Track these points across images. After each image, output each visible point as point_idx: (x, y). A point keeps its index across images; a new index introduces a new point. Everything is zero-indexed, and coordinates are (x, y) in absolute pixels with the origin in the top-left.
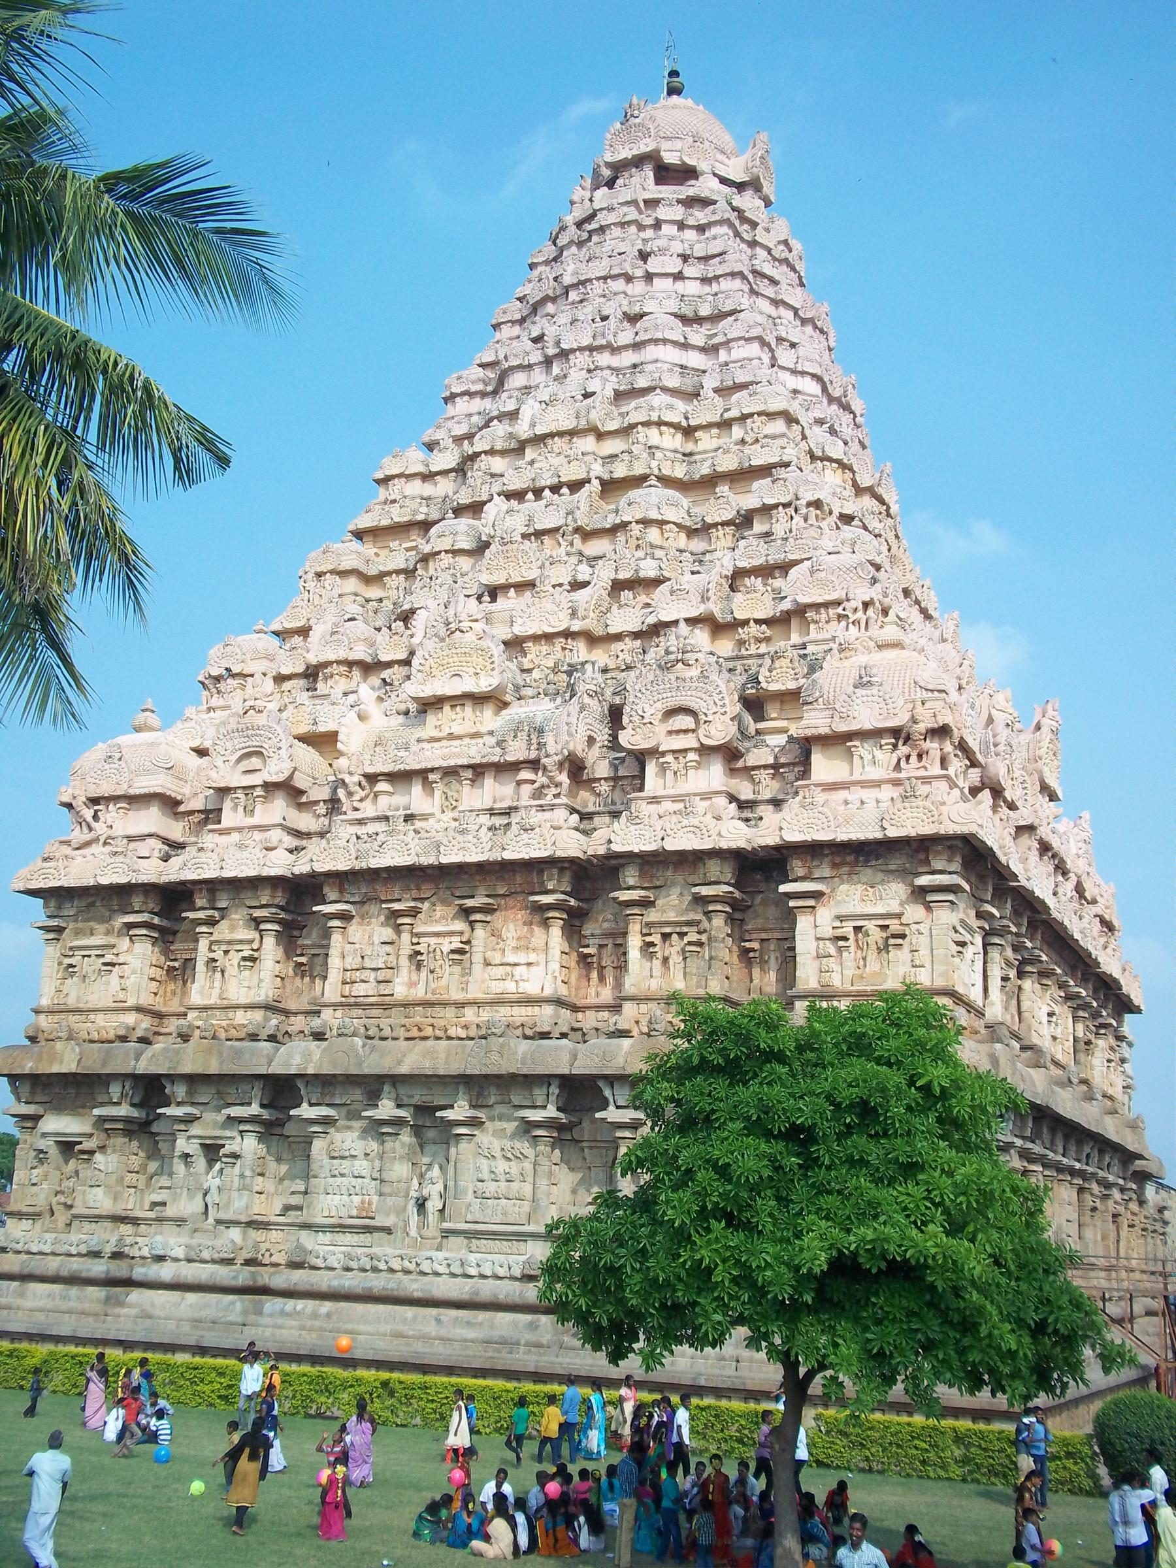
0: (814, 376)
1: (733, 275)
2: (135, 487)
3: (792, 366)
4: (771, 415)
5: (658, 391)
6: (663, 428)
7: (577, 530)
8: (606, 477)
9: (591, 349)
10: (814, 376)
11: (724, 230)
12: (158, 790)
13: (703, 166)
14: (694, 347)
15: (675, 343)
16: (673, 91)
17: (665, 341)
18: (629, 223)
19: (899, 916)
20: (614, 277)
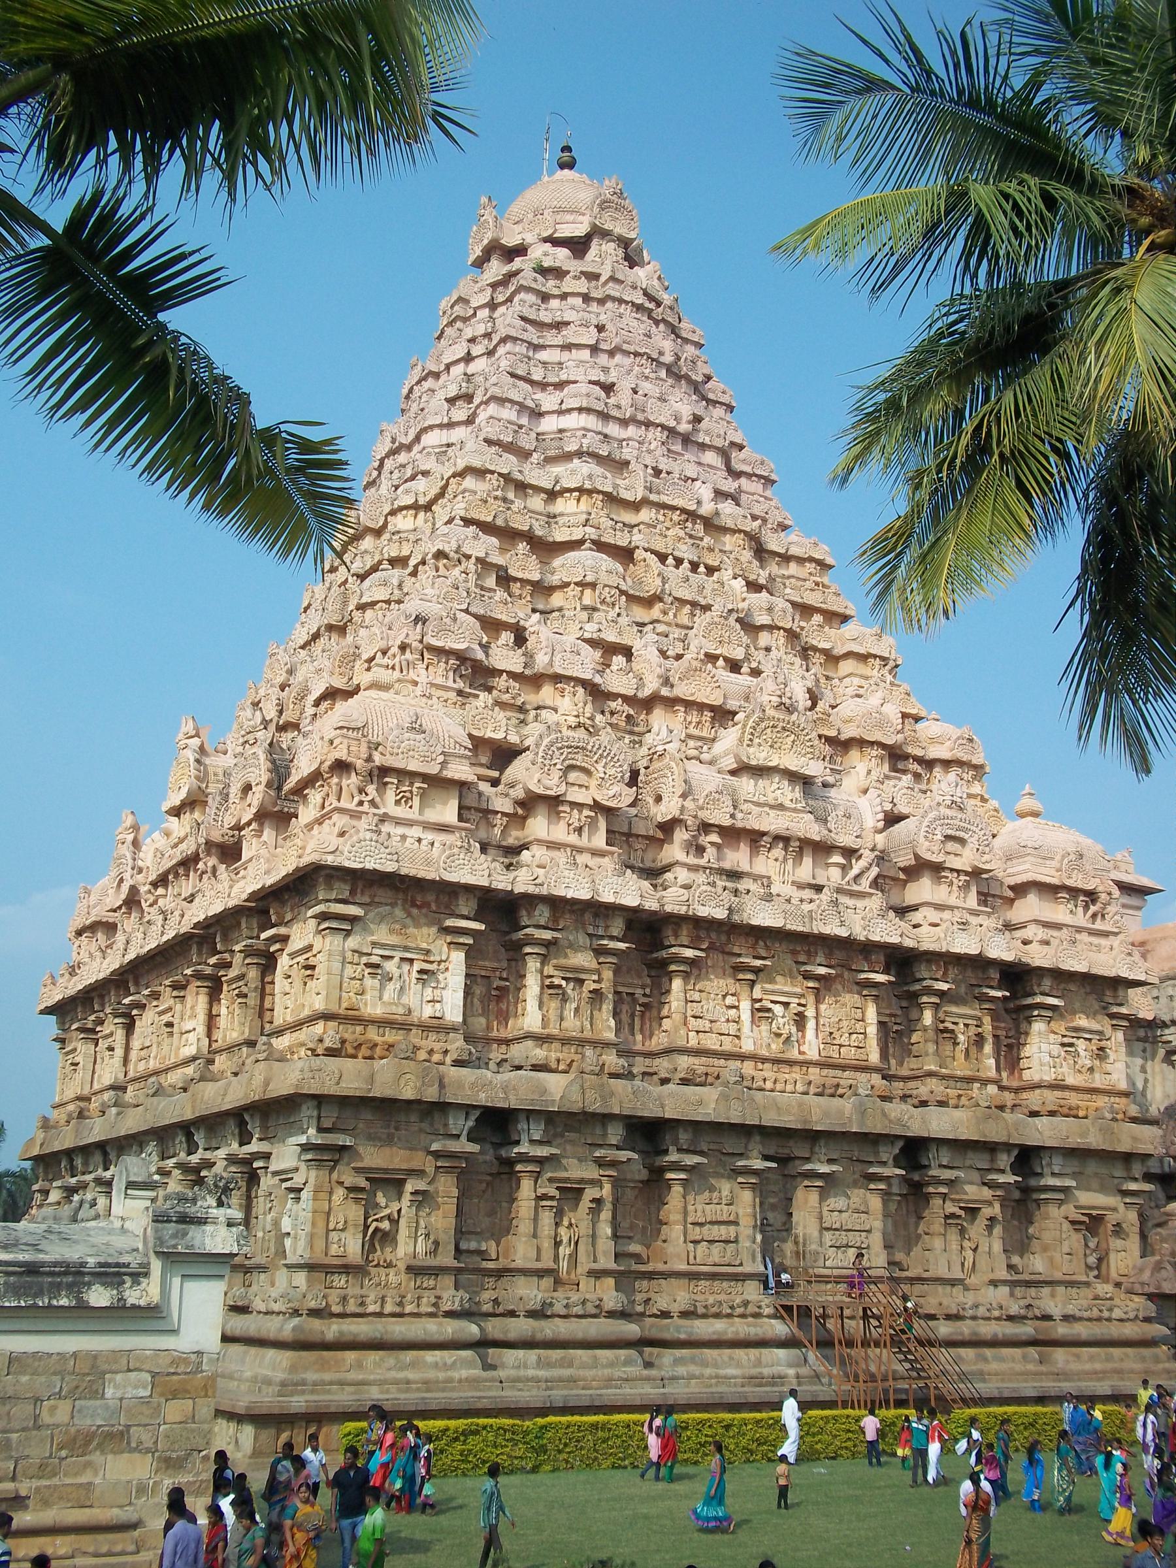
0: (580, 410)
1: (504, 340)
2: (876, 573)
3: (556, 407)
4: (461, 474)
5: (420, 476)
6: (404, 512)
7: (330, 628)
8: (362, 571)
9: (393, 452)
10: (580, 410)
11: (522, 295)
12: (98, 919)
13: (530, 238)
14: (459, 424)
15: (441, 426)
16: (562, 166)
17: (431, 427)
18: (454, 321)
19: (309, 948)
20: (424, 379)
